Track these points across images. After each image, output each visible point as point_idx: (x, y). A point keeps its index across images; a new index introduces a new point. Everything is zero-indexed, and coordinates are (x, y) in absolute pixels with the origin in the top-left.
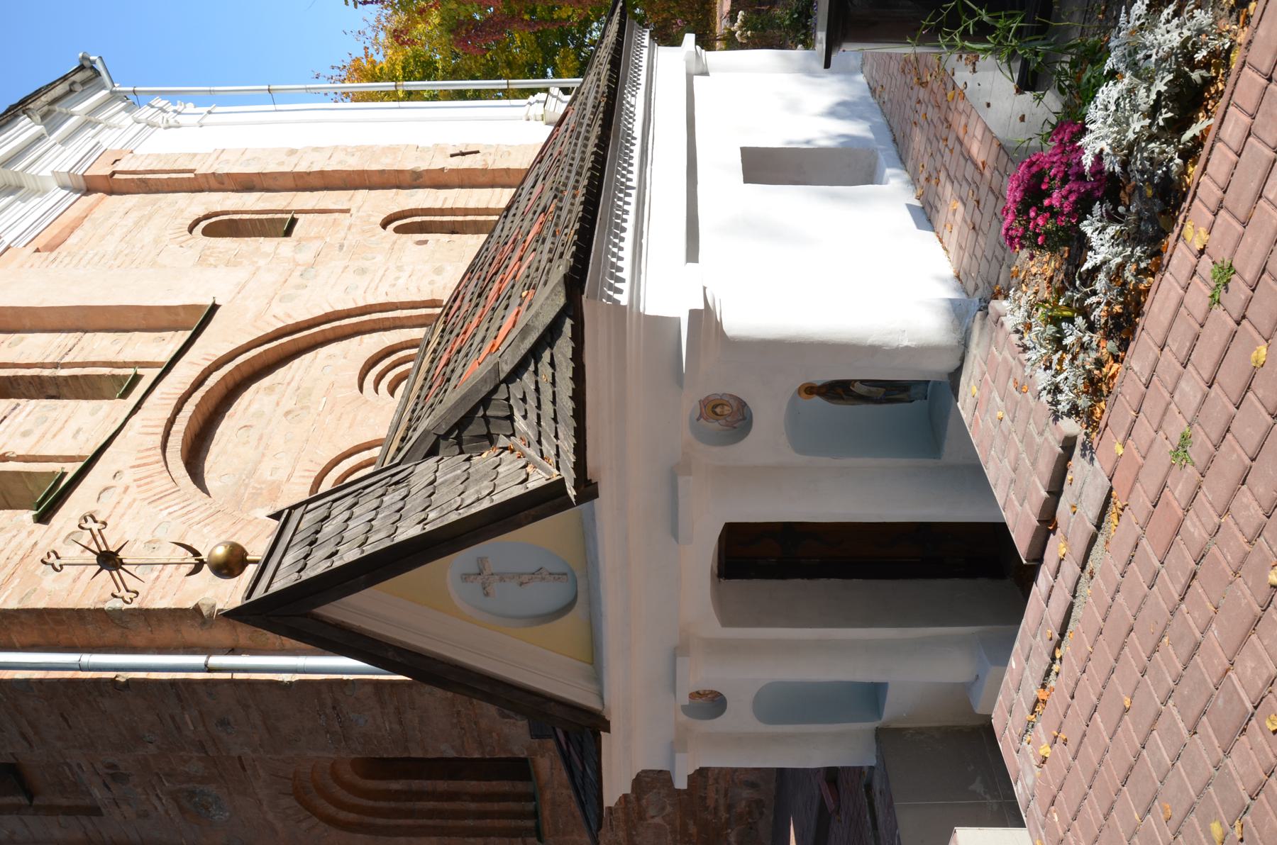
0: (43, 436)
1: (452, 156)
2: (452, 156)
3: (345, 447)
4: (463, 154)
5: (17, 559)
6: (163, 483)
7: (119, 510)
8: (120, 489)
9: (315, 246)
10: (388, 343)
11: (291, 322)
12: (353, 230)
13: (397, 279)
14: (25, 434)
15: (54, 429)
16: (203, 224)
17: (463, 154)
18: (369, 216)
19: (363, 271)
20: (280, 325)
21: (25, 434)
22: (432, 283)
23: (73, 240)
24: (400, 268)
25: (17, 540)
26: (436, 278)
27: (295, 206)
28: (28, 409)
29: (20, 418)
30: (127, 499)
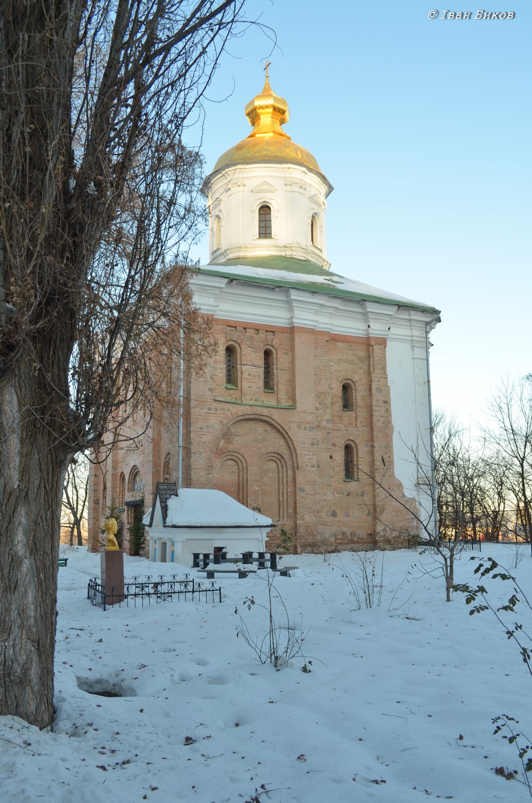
0: (248, 379)
1: (382, 458)
2: (382, 458)
3: (245, 456)
4: (383, 461)
5: (204, 400)
6: (226, 421)
7: (217, 415)
8: (224, 413)
9: (329, 425)
10: (284, 457)
11: (288, 431)
12: (345, 432)
13: (309, 455)
14: (249, 375)
15: (251, 381)
16: (350, 382)
17: (383, 461)
18: (353, 435)
19: (313, 444)
20: (286, 429)
21: (249, 375)
22: (307, 465)
23: (339, 344)
24: (313, 455)
25: (209, 397)
26: (309, 466)
27: (358, 409)
28: (259, 371)
29: (255, 370)
30: (220, 416)
